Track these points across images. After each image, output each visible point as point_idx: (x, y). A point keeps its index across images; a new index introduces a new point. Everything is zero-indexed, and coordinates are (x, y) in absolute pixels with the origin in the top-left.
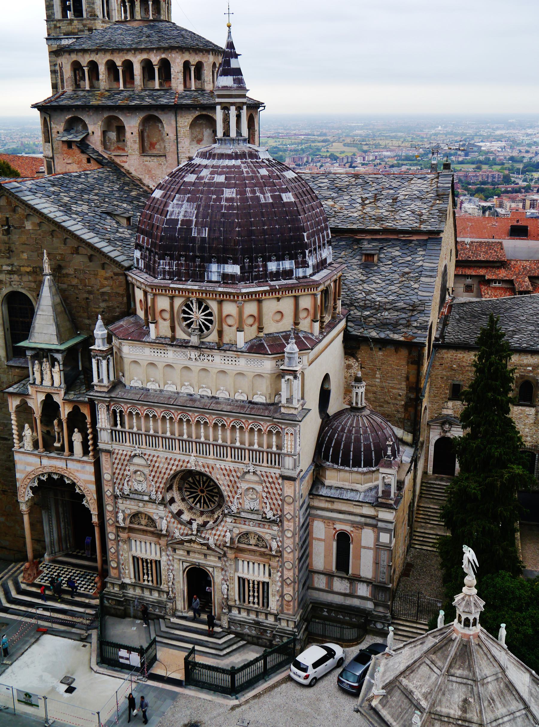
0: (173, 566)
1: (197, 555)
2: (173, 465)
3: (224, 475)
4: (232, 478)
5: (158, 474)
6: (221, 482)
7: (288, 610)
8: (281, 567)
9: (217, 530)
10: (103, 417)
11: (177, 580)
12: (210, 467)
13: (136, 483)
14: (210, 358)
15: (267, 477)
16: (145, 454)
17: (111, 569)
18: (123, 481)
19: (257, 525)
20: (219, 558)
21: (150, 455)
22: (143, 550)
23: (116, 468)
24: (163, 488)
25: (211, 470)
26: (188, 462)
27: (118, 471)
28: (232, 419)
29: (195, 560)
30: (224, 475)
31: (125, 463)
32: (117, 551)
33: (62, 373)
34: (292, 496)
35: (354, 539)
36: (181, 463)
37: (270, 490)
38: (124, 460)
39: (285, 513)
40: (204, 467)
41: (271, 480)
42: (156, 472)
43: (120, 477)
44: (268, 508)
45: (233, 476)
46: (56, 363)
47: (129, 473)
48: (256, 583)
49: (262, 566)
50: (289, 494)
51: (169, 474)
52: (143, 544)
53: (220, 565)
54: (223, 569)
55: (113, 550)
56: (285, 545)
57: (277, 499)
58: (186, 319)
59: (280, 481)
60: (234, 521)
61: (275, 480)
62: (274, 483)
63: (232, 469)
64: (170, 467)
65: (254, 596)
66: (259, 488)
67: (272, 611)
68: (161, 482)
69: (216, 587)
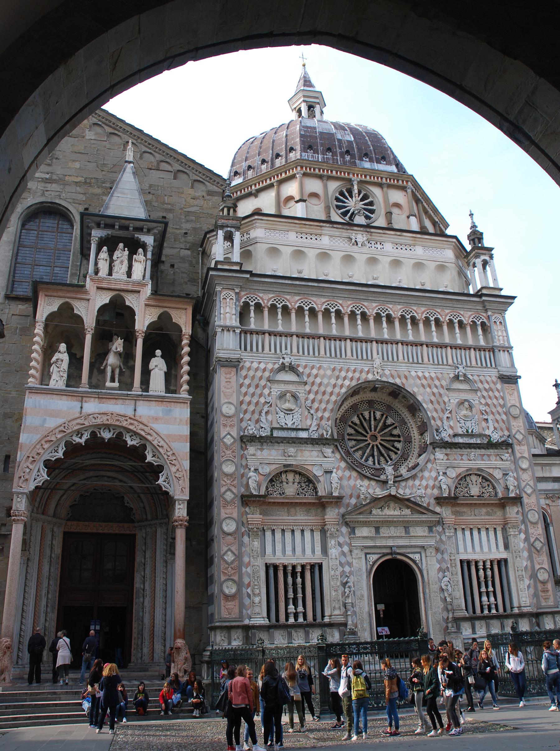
0: (350, 564)
1: (392, 531)
2: (345, 378)
3: (423, 386)
4: (435, 390)
5: (319, 397)
6: (420, 398)
7: (546, 599)
8: (523, 522)
9: (422, 478)
10: (228, 310)
11: (358, 593)
12: (402, 376)
13: (282, 414)
14: (378, 246)
15: (481, 382)
16: (298, 366)
17: (222, 602)
18: (256, 416)
19: (480, 457)
20: (430, 529)
21: (306, 367)
22: (289, 548)
23: (245, 394)
24: (328, 419)
25: (404, 380)
26: (368, 372)
27: (247, 399)
28: (423, 309)
29: (390, 543)
30: (423, 386)
31: (263, 382)
32: (239, 557)
33: (149, 263)
34: (518, 405)
35: (553, 517)
36: (357, 375)
37: (489, 401)
38: (261, 378)
39: (514, 432)
40: (392, 376)
41: (487, 386)
42: (317, 393)
43: (252, 408)
44: (492, 429)
45: (436, 387)
46: (140, 250)
47: (269, 399)
48: (488, 565)
49: (491, 533)
50: (513, 402)
51: (338, 394)
52: (288, 535)
53: (432, 542)
54: (437, 550)
55: (229, 557)
56: (523, 484)
57: (499, 414)
58: (339, 207)
59: (499, 386)
60: (446, 457)
61: (492, 385)
62: (492, 390)
63: (433, 375)
64: (340, 382)
65: (488, 593)
66: (474, 398)
67: (525, 610)
68: (325, 410)
69: (427, 591)
